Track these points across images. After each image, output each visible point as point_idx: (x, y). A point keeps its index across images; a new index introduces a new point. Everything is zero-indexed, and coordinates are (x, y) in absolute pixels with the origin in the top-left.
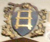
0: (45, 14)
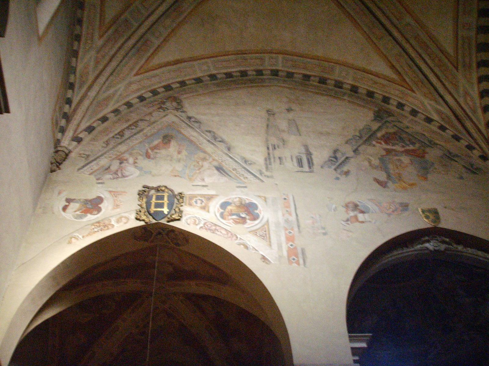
0: (182, 198)
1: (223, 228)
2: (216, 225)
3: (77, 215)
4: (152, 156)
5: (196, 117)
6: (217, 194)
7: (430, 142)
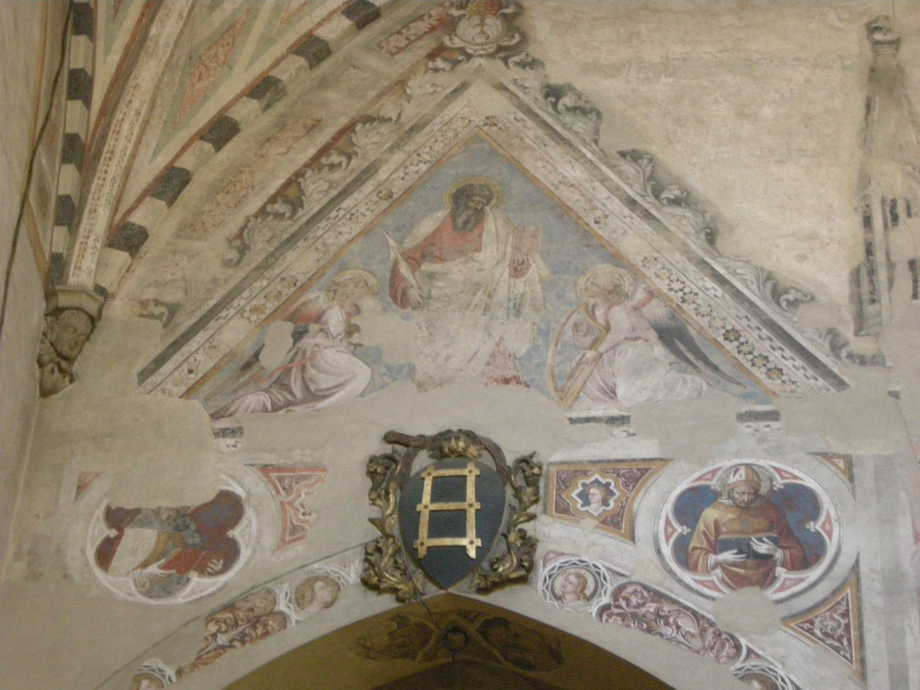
0: (532, 481)
1: (687, 608)
2: (658, 596)
3: (154, 579)
4: (414, 294)
5: (578, 86)
6: (662, 457)
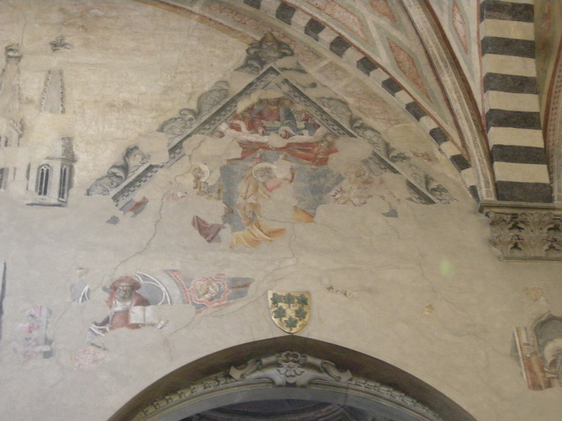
7: (352, 121)
